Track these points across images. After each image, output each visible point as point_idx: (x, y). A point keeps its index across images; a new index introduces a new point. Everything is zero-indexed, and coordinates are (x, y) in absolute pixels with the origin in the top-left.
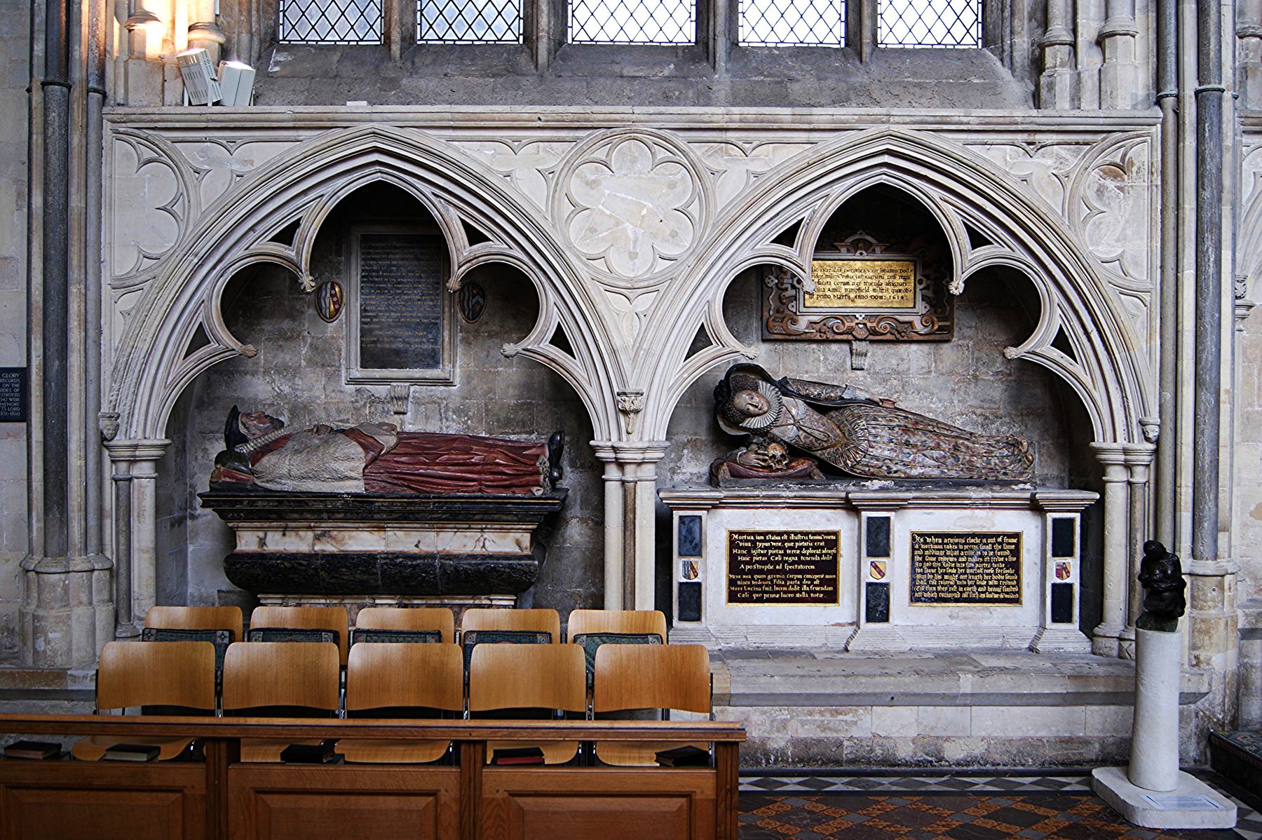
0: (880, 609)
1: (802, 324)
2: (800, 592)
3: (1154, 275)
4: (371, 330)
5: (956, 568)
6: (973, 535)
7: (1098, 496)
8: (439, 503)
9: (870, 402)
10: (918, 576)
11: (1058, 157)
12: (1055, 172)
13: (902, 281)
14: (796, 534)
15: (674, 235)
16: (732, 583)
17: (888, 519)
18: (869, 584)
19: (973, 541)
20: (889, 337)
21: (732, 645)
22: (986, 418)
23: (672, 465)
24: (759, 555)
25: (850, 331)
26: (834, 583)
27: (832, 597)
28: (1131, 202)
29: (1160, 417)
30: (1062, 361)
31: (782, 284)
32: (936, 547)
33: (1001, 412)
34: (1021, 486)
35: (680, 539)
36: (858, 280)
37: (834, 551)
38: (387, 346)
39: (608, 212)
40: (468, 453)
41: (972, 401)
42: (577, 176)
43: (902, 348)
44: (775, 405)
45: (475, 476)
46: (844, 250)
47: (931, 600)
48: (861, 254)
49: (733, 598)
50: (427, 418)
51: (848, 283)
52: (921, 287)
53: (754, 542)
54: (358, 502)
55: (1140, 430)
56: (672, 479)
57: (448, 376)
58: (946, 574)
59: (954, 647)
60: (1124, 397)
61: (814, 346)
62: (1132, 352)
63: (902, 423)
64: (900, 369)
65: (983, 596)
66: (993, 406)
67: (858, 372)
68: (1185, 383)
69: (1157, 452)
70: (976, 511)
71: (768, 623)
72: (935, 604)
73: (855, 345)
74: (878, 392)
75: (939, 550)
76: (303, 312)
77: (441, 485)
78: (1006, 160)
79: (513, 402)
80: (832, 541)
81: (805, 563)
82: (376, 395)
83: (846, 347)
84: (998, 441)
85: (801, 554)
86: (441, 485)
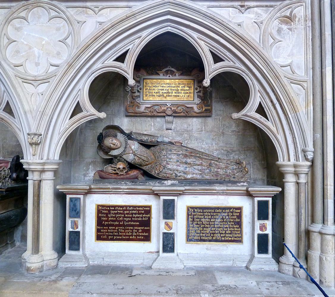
0: (170, 246)
1: (142, 109)
2: (132, 235)
3: (309, 73)
5: (209, 224)
6: (218, 208)
7: (280, 189)
9: (171, 143)
10: (191, 228)
11: (257, 13)
12: (255, 21)
13: (188, 88)
14: (130, 206)
15: (58, 54)
16: (98, 231)
17: (173, 200)
18: (164, 233)
19: (217, 211)
20: (182, 114)
21: (96, 263)
22: (228, 152)
23: (84, 172)
24: (112, 217)
25: (164, 112)
26: (149, 231)
27: (147, 239)
28: (295, 36)
29: (314, 147)
30: (260, 119)
31: (133, 90)
32: (199, 214)
33: (235, 149)
34: (242, 184)
35: (70, 209)
36: (168, 88)
37: (149, 215)
39: (25, 43)
41: (221, 144)
42: (11, 25)
43: (189, 120)
44: (124, 144)
46: (161, 75)
47: (197, 240)
48: (169, 76)
49: (99, 238)
51: (163, 90)
52: (197, 91)
53: (109, 211)
55: (303, 155)
56: (84, 179)
58: (205, 227)
59: (208, 265)
60: (294, 138)
61: (149, 119)
62: (298, 113)
63: (184, 153)
64: (189, 129)
65: (223, 239)
66: (231, 146)
67: (169, 131)
68: (328, 128)
69: (312, 166)
70: (219, 196)
71: (116, 251)
72: (199, 243)
73: (167, 118)
74: (178, 139)
75: (201, 215)
78: (229, 15)
80: (147, 210)
81: (134, 221)
83: (163, 119)
84: (232, 162)
85: (132, 217)
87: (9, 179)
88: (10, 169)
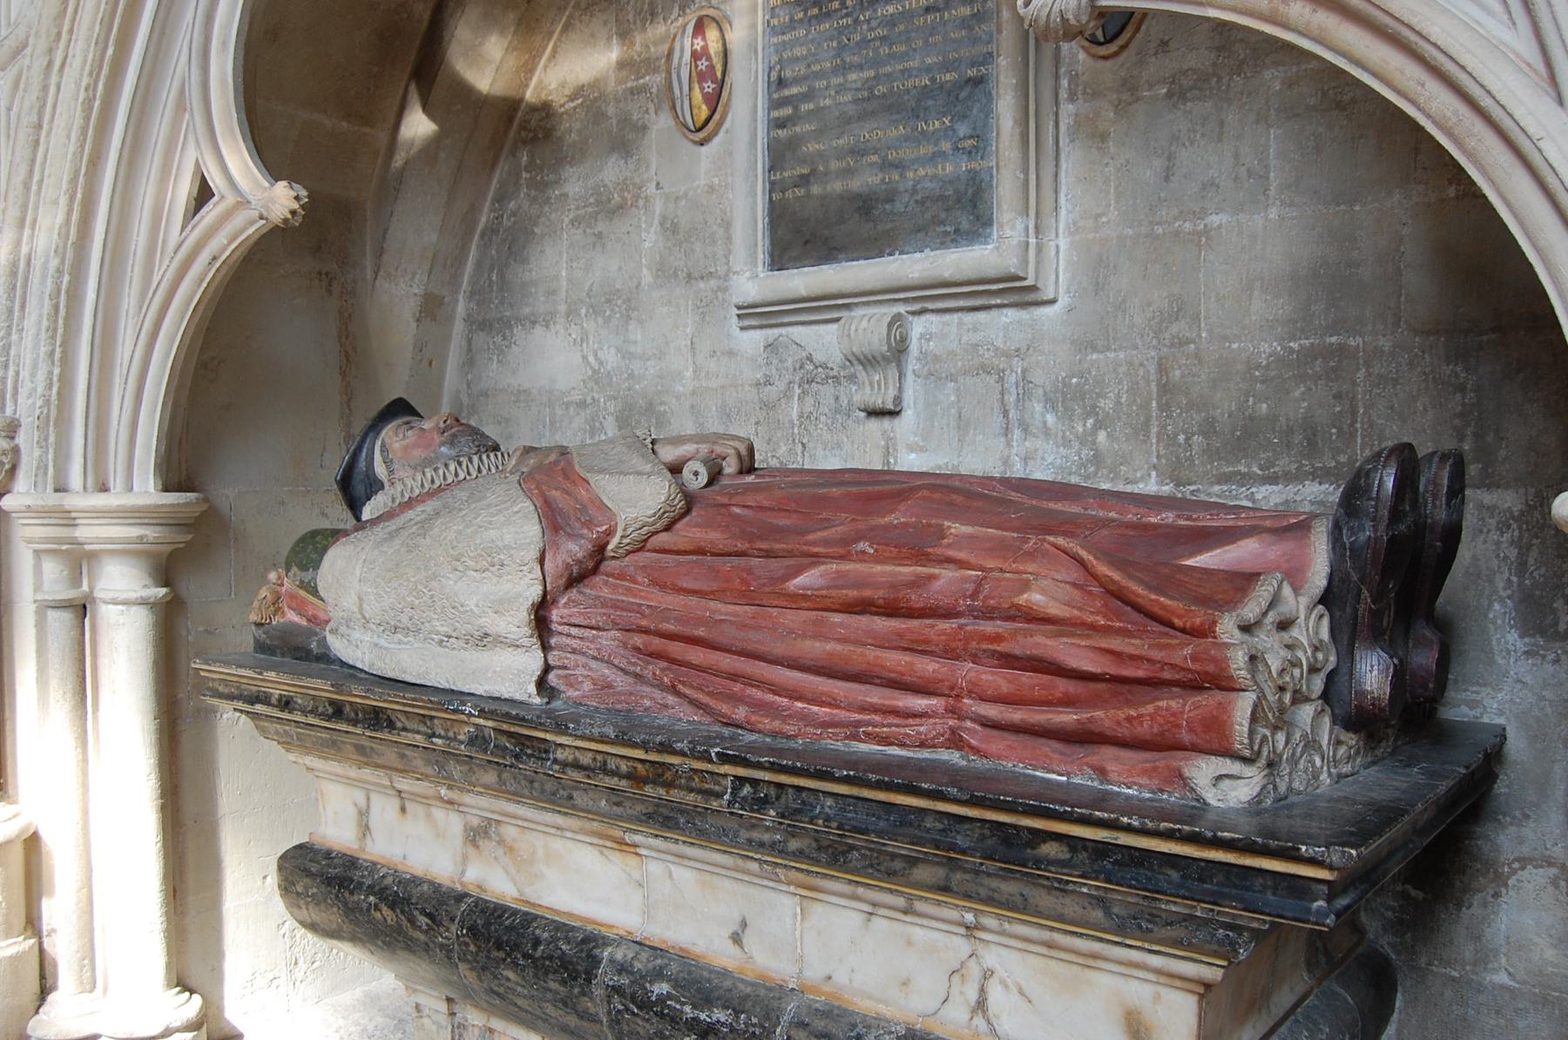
4: (793, 144)
8: (755, 783)
38: (837, 186)
40: (922, 557)
45: (928, 667)
50: (962, 424)
54: (510, 735)
57: (1011, 264)
76: (644, 128)
77: (795, 695)
79: (1267, 348)
82: (819, 357)
86: (795, 695)
87: (1318, 714)
88: (1326, 599)
